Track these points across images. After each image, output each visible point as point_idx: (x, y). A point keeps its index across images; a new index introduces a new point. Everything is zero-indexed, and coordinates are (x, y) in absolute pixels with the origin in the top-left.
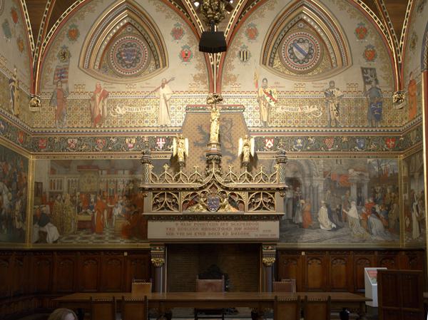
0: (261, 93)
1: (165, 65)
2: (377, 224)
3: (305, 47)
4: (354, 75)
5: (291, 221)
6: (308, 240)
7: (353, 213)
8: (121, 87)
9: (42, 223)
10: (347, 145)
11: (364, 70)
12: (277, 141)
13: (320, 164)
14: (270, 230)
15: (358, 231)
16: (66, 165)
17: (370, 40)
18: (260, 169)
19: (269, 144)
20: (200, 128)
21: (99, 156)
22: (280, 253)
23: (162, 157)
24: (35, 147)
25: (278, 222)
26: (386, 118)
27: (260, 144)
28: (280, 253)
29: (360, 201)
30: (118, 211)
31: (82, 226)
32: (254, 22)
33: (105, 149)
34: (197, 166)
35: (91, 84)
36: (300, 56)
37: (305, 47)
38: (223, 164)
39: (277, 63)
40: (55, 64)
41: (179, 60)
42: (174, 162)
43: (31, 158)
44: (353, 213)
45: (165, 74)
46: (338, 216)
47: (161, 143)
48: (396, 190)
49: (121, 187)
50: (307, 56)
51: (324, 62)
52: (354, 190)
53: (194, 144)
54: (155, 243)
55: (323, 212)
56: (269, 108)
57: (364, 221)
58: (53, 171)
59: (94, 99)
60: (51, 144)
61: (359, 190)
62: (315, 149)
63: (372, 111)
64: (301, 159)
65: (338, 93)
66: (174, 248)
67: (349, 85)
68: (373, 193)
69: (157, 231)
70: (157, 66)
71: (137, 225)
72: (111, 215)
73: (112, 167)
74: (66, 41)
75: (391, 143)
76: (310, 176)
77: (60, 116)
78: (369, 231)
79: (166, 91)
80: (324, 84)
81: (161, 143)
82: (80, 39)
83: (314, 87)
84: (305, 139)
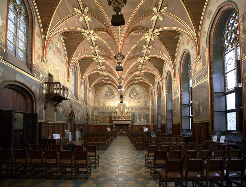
0: (129, 101)
1: (114, 97)
2: (146, 121)
3: (136, 93)
4: (142, 99)
5: (133, 121)
6: (136, 124)
7: (142, 120)
8: (108, 100)
9: (97, 121)
10: (141, 109)
11: (144, 98)
12: (131, 109)
13: (138, 112)
14: (130, 122)
15: (143, 122)
16: (100, 112)
17: (145, 93)
18: (128, 114)
19: (130, 109)
20: (120, 107)
21: (104, 111)
22: (131, 126)
23: (114, 111)
24: (95, 109)
25: (131, 121)
26: (147, 105)
27: (128, 109)
28: (131, 125)
29: (143, 118)
30: (108, 119)
31: (103, 121)
32: (128, 90)
33: (106, 110)
34: (120, 113)
35: (103, 100)
36: (135, 95)
37: (136, 93)
38: (123, 113)
39: (131, 96)
40: (98, 97)
41: (116, 96)
42: (116, 112)
43: (95, 111)
44: (142, 120)
45: (114, 98)
46: (140, 120)
47: (114, 109)
48: (148, 116)
49: (108, 116)
50: (136, 95)
51: (139, 96)
52: (142, 116)
53: (119, 110)
54: (114, 124)
55: (138, 119)
56: (130, 104)
57: (144, 121)
58: (98, 113)
59: (104, 102)
60: (97, 109)
61: (143, 116)
62: (137, 110)
63: (145, 104)
64: (135, 111)
65: (140, 101)
66: (116, 125)
67: (142, 100)
68: (145, 117)
69: (114, 122)
70: (113, 97)
71: (111, 121)
72: (107, 120)
73: (107, 113)
74: (99, 93)
75: (148, 109)
76: (136, 114)
77: (99, 105)
78: (144, 122)
79: (115, 101)
80: (138, 100)
81: (114, 109)
82: (102, 93)
83: (137, 101)
84: (135, 108)
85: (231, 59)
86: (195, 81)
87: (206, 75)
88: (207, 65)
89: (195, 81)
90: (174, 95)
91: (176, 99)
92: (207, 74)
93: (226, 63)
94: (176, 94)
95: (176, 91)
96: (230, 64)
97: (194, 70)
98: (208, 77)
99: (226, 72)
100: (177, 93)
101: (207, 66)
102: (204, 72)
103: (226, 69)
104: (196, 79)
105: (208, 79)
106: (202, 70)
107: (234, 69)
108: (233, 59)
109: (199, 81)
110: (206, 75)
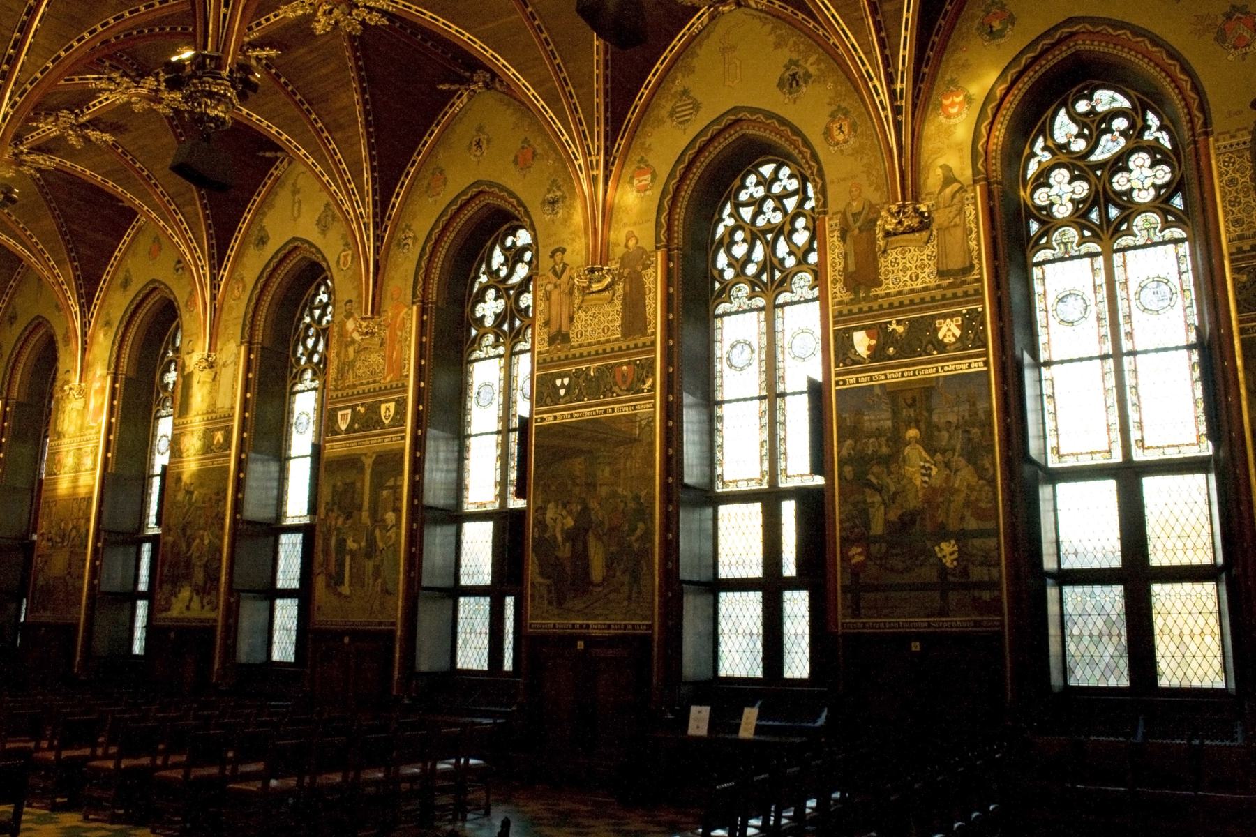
85: (748, 350)
86: (562, 392)
87: (646, 386)
88: (654, 334)
89: (562, 392)
90: (343, 427)
91: (368, 462)
92: (649, 382)
93: (718, 353)
94: (366, 427)
95: (374, 409)
96: (742, 369)
97: (554, 329)
98: (653, 397)
99: (719, 399)
100: (379, 422)
101: (653, 343)
102: (628, 364)
103: (718, 381)
104: (566, 381)
105: (654, 406)
106: (611, 345)
107: (761, 398)
108: (753, 351)
109: (586, 401)
110: (646, 386)
